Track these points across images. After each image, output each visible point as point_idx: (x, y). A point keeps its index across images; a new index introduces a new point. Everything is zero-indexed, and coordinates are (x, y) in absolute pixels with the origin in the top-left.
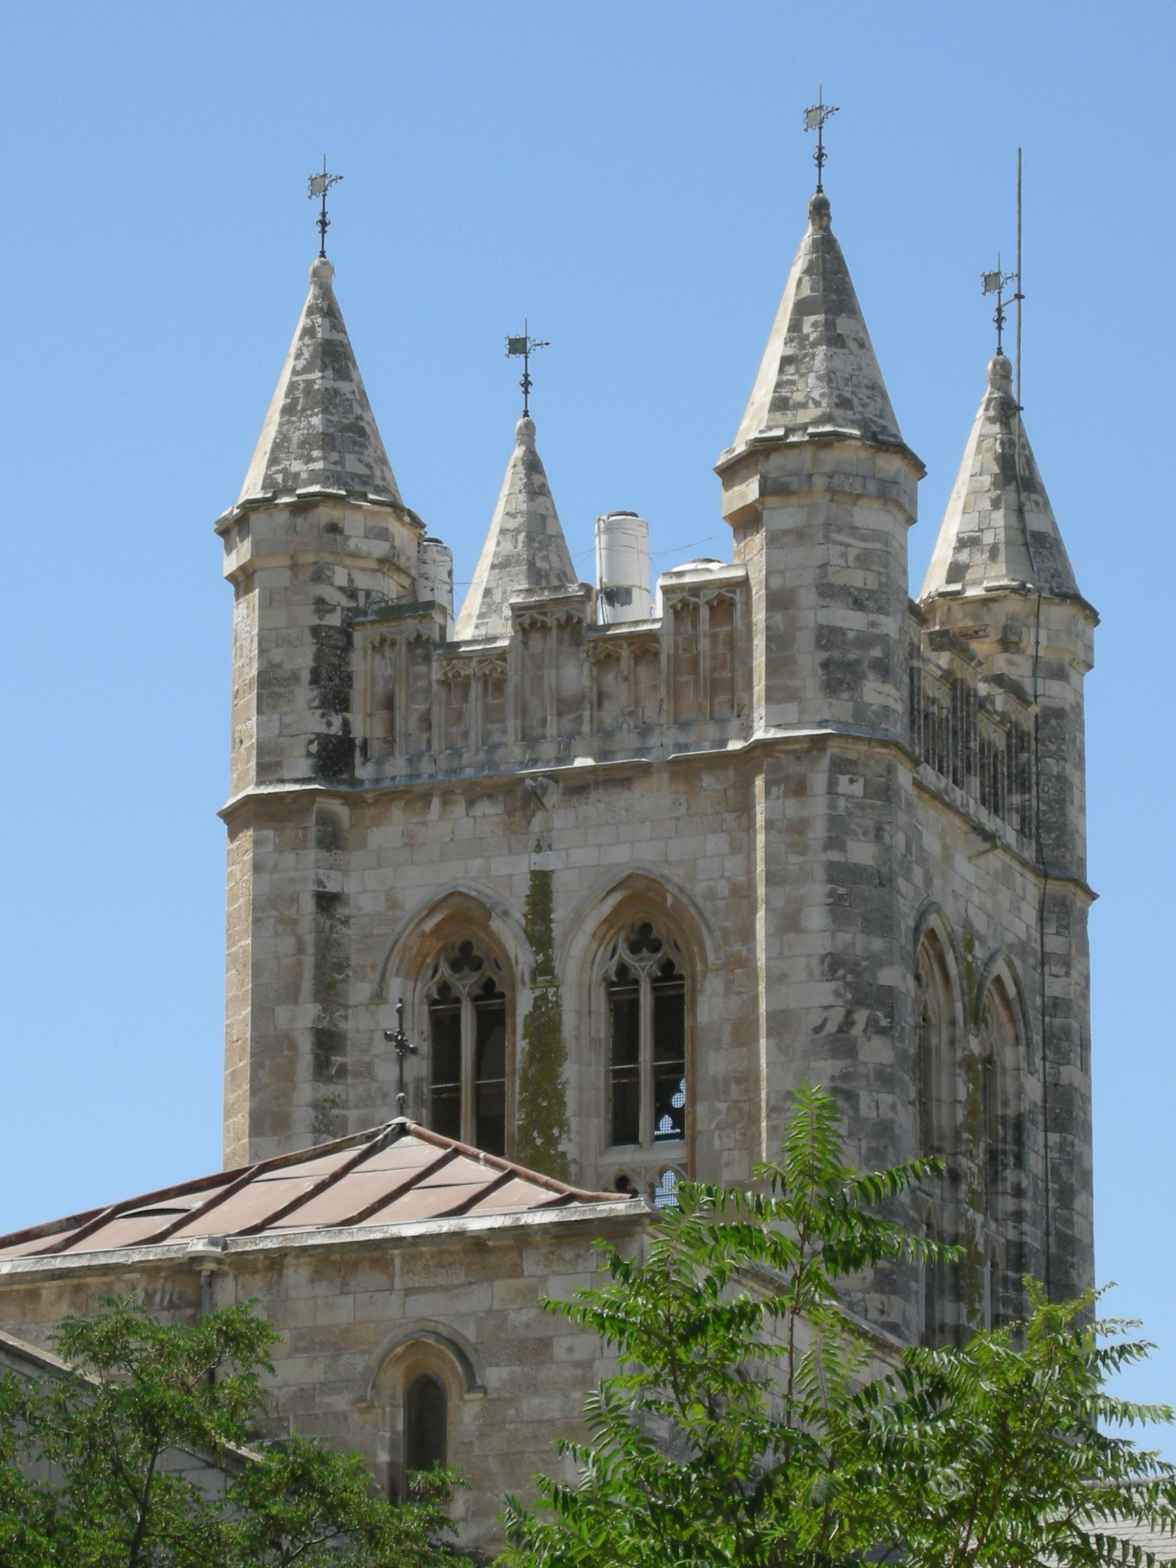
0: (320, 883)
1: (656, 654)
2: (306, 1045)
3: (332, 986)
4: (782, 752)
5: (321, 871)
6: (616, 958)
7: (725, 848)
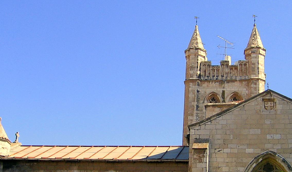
1: (237, 69)
2: (195, 107)
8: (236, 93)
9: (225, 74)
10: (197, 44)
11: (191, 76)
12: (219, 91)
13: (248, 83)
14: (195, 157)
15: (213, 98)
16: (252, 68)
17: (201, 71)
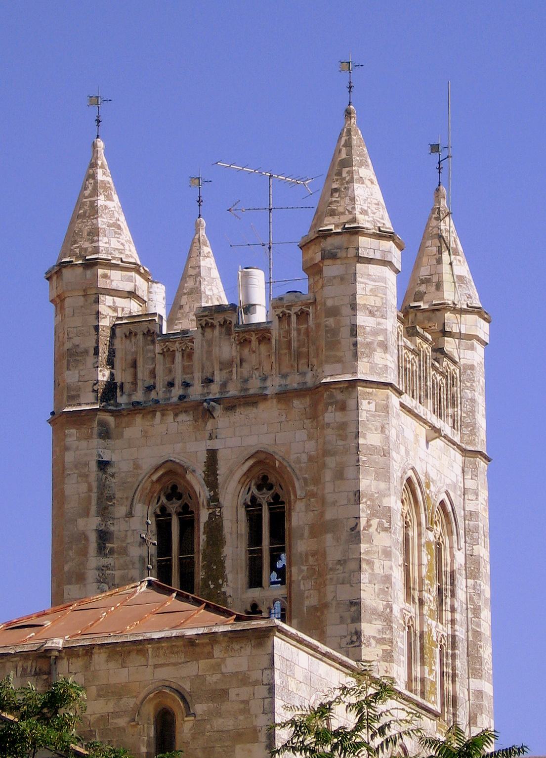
0: (100, 456)
1: (269, 339)
2: (93, 537)
3: (106, 508)
4: (333, 389)
5: (100, 450)
6: (250, 493)
7: (305, 438)
8: (262, 456)
9: (217, 373)
10: (96, 238)
11: (73, 398)
13: (314, 405)
15: (174, 487)
17: (117, 362)
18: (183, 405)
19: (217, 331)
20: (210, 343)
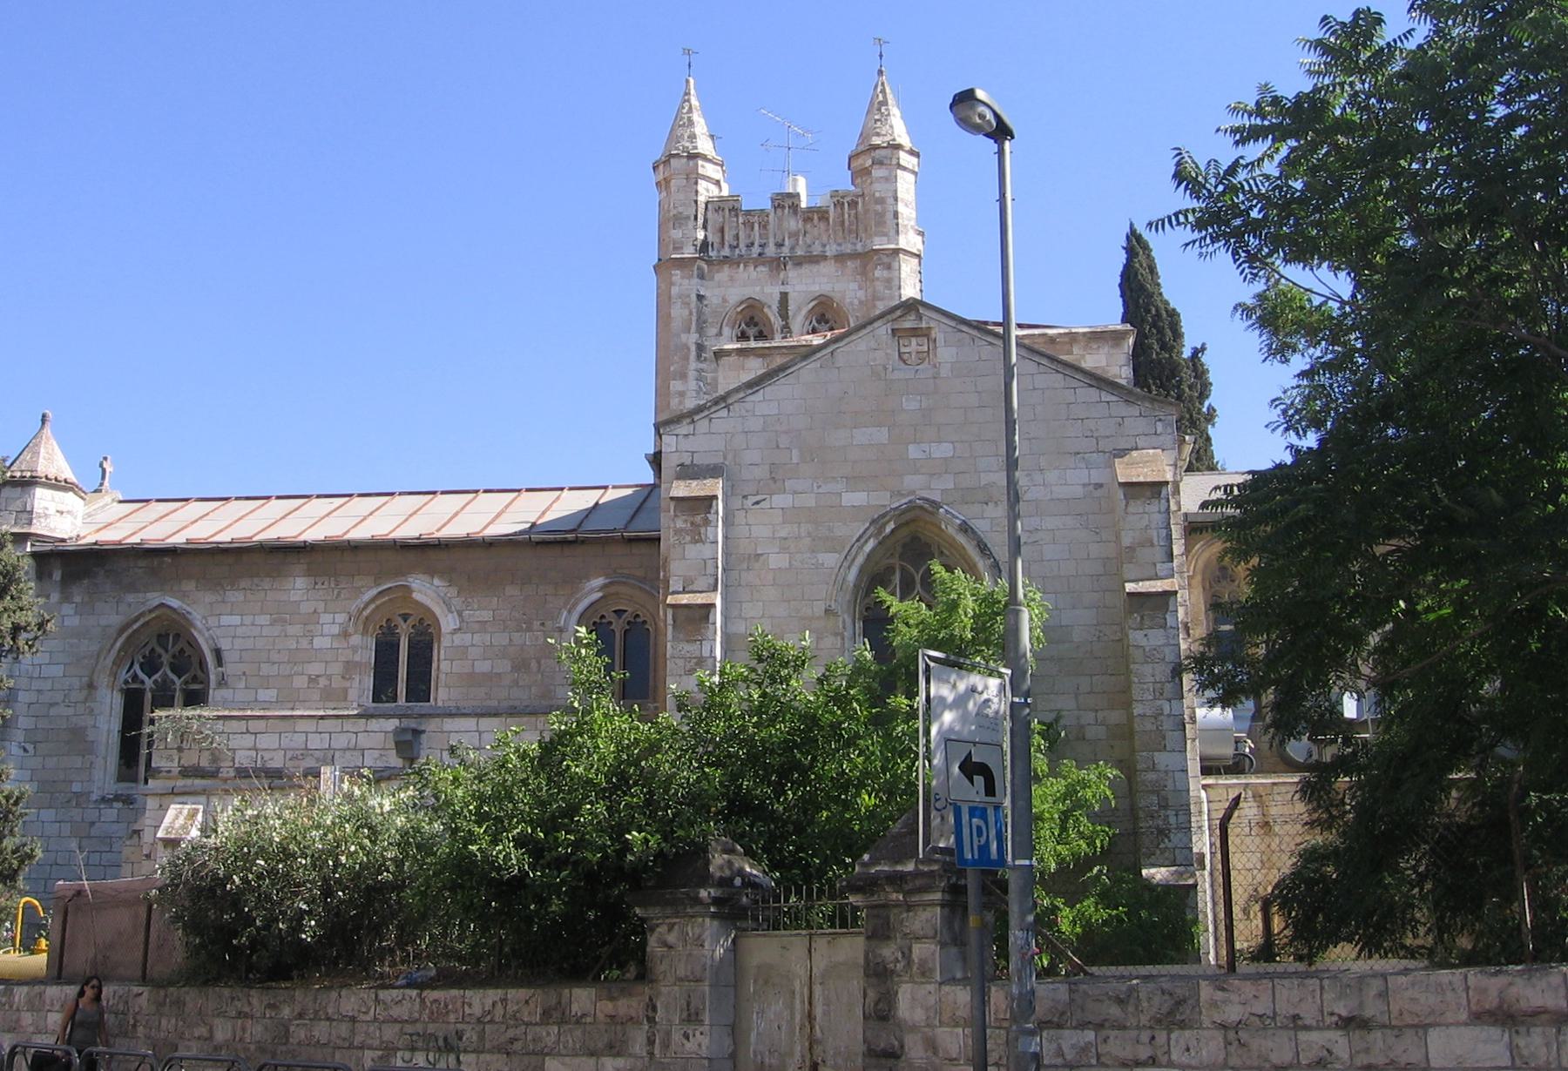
1: (827, 219)
2: (693, 348)
3: (702, 328)
11: (678, 249)
12: (769, 293)
13: (864, 266)
14: (680, 524)
15: (752, 318)
16: (877, 213)
17: (709, 228)
18: (761, 259)
19: (787, 210)
20: (780, 219)
